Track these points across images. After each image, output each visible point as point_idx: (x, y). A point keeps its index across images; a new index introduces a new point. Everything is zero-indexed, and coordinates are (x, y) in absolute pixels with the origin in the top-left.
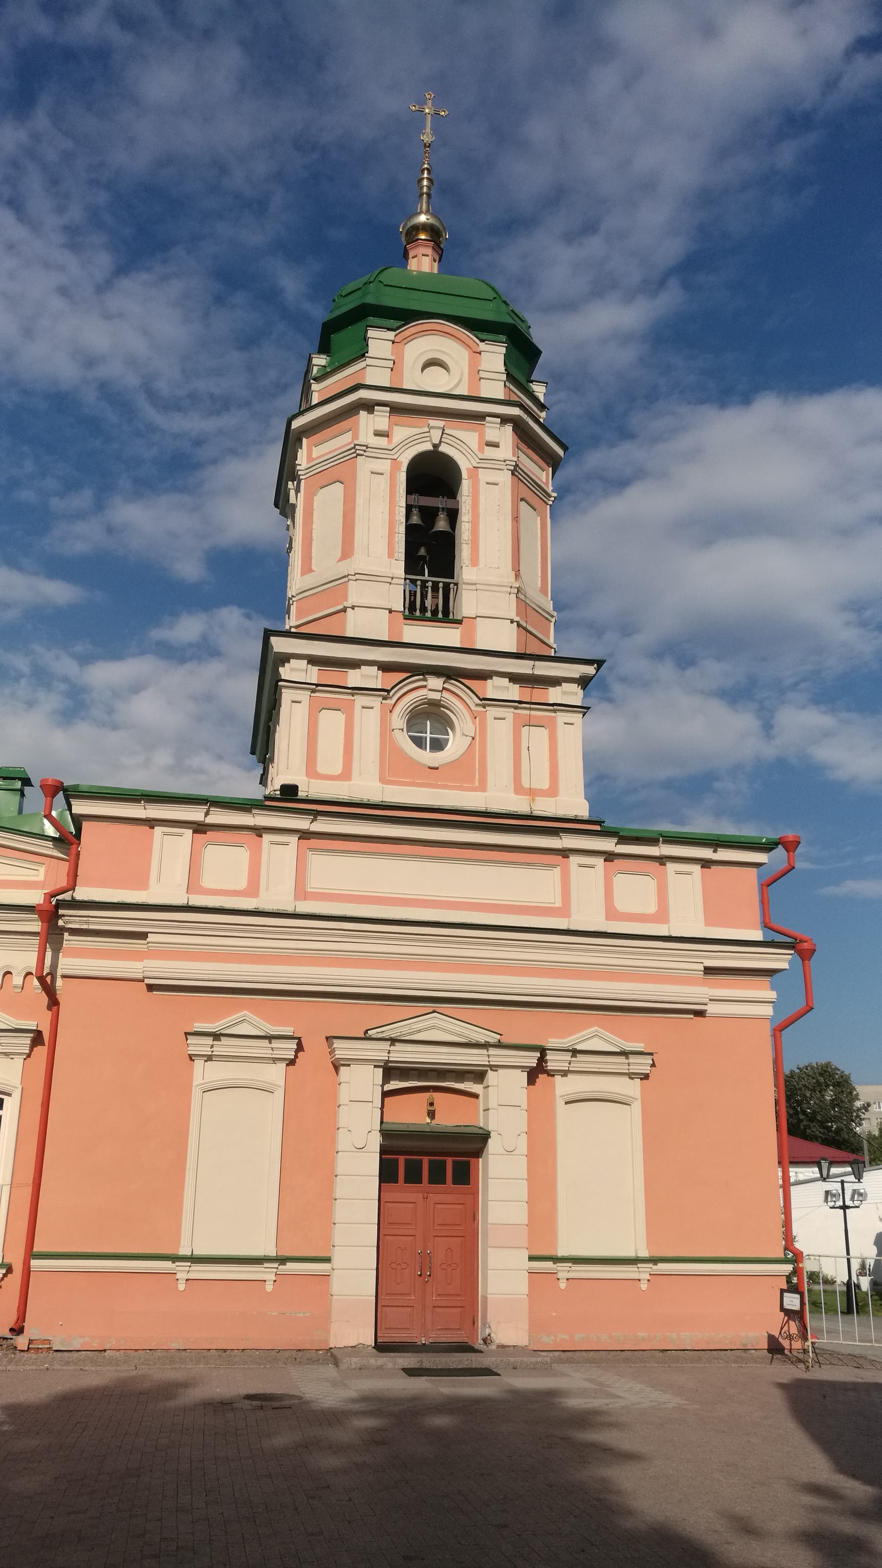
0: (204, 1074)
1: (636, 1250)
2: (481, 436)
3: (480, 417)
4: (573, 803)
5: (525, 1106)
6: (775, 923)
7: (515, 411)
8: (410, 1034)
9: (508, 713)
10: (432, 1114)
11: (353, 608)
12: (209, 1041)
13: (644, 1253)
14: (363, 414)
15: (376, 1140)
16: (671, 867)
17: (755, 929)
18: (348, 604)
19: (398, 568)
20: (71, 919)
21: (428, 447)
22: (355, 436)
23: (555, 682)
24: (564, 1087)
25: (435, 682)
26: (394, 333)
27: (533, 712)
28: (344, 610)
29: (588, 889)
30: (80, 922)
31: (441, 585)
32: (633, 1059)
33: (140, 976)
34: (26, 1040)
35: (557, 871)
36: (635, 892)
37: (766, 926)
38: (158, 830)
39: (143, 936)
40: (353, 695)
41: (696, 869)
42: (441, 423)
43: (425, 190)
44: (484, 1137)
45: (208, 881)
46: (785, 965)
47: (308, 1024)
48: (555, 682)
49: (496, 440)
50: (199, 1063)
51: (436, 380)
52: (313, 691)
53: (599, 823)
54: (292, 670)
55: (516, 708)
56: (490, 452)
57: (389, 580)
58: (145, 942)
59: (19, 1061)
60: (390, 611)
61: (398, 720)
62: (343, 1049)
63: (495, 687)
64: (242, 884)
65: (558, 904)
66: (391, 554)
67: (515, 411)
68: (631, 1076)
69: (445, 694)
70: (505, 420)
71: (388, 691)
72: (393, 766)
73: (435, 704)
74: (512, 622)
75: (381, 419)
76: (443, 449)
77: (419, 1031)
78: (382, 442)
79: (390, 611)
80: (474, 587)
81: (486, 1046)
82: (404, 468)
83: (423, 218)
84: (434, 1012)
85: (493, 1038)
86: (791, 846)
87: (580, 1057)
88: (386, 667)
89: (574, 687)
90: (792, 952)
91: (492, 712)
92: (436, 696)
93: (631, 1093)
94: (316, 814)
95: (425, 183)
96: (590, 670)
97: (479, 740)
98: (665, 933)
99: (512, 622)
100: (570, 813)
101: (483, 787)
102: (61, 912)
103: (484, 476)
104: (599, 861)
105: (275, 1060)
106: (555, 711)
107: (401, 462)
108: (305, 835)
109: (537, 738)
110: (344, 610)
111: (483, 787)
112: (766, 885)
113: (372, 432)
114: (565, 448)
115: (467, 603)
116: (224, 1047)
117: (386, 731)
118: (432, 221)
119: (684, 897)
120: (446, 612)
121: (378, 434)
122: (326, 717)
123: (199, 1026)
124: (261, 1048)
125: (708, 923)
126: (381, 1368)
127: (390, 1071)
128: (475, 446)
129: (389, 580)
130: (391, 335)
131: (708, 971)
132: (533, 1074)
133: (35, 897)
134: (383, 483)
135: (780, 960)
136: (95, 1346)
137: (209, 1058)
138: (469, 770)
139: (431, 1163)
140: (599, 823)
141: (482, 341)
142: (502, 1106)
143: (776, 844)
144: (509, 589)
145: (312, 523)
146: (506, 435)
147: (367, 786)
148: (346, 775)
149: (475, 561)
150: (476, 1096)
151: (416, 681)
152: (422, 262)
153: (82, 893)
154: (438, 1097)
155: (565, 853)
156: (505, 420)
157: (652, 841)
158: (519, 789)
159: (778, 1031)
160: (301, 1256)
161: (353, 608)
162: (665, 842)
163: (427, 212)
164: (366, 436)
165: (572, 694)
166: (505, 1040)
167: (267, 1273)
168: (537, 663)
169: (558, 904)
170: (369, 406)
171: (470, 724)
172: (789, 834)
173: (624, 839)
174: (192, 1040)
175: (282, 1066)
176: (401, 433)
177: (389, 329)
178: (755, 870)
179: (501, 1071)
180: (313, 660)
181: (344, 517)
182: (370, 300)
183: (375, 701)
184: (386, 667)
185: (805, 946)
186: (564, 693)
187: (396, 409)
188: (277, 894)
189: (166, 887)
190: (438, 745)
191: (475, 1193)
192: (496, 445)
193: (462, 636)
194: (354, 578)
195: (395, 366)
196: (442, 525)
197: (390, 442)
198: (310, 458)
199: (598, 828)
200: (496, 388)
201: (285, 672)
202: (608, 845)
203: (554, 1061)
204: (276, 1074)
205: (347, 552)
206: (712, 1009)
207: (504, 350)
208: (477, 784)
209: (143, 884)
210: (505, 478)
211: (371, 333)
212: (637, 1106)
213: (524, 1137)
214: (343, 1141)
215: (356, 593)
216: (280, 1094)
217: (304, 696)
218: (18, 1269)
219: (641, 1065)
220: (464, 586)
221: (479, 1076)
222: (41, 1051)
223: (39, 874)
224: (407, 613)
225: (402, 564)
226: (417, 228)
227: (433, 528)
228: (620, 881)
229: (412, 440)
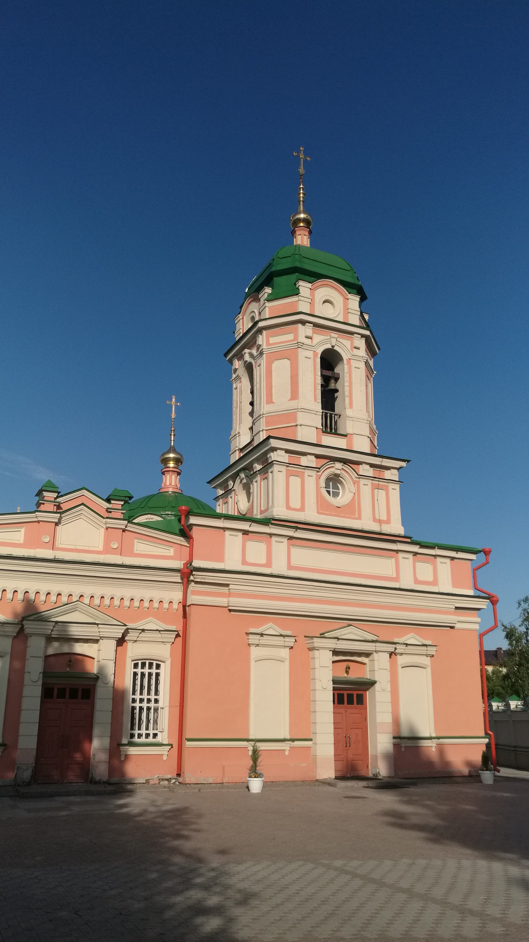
0: (255, 652)
1: (430, 734)
2: (352, 343)
3: (352, 333)
4: (396, 527)
5: (389, 670)
6: (479, 586)
7: (367, 333)
8: (342, 635)
9: (369, 482)
10: (347, 672)
11: (301, 425)
12: (258, 637)
13: (434, 735)
14: (300, 325)
15: (331, 686)
16: (439, 560)
17: (471, 589)
18: (299, 423)
19: (318, 407)
20: (198, 576)
21: (329, 346)
22: (296, 337)
23: (388, 468)
24: (401, 660)
25: (338, 465)
26: (311, 285)
27: (380, 483)
28: (296, 426)
29: (409, 569)
30: (201, 578)
31: (329, 414)
32: (429, 648)
33: (226, 605)
34: (173, 635)
35: (393, 559)
36: (425, 570)
37: (476, 588)
38: (227, 533)
39: (227, 585)
40: (304, 469)
41: (448, 561)
42: (336, 336)
43: (302, 199)
44: (372, 683)
45: (249, 559)
46: (485, 607)
47: (304, 630)
48: (388, 468)
49: (359, 346)
50: (253, 648)
51: (328, 311)
52: (288, 466)
53: (410, 538)
54: (278, 455)
55: (372, 480)
56: (356, 352)
57: (316, 413)
58: (227, 588)
59: (169, 646)
60: (317, 428)
61: (323, 484)
62: (318, 642)
63: (364, 470)
64: (264, 561)
65: (395, 576)
66: (315, 400)
67: (367, 333)
68: (427, 655)
69: (342, 472)
70: (363, 336)
71: (319, 468)
72: (323, 507)
73: (337, 476)
74: (368, 437)
75: (308, 330)
76: (336, 348)
77: (345, 635)
78: (308, 341)
79: (317, 428)
80: (351, 419)
81: (373, 641)
82: (319, 357)
83: (302, 216)
84: (351, 625)
85: (375, 638)
86: (487, 553)
87: (409, 647)
88: (318, 456)
89: (396, 471)
90: (488, 601)
91: (362, 481)
92: (338, 472)
93: (426, 663)
94: (297, 528)
95: (302, 195)
96: (404, 464)
97: (357, 494)
98: (437, 591)
99: (368, 437)
100: (393, 532)
101: (359, 518)
102: (194, 573)
103: (354, 363)
104: (410, 556)
105: (285, 647)
106: (388, 482)
107: (318, 353)
108: (291, 538)
109: (382, 494)
110: (296, 426)
111: (359, 518)
112: (475, 570)
113: (304, 336)
114: (379, 349)
115: (348, 426)
116: (265, 640)
117: (318, 488)
118: (305, 216)
119: (443, 573)
120: (336, 430)
121: (307, 337)
122: (292, 478)
123: (252, 630)
124: (280, 641)
125: (454, 586)
126: (352, 787)
127: (335, 653)
128: (349, 348)
129: (316, 413)
130: (310, 285)
131: (457, 608)
132: (391, 654)
133: (178, 564)
134: (310, 362)
135: (483, 604)
136: (218, 781)
137: (258, 645)
138: (352, 509)
139: (350, 695)
140: (410, 538)
141: (350, 293)
142: (378, 668)
143: (481, 551)
144: (366, 421)
145: (272, 377)
146: (361, 343)
147: (311, 515)
148: (302, 509)
149: (351, 406)
150: (364, 664)
151: (331, 464)
152: (302, 239)
153: (196, 563)
154: (350, 664)
155: (397, 551)
156: (363, 336)
157: (432, 548)
158: (375, 520)
159: (481, 636)
160: (301, 737)
161: (301, 425)
162: (438, 548)
163: (304, 212)
164: (302, 339)
165: (393, 475)
166: (380, 639)
167: (286, 747)
168: (384, 459)
169: (395, 576)
170: (303, 322)
171: (353, 486)
172: (487, 547)
173: (422, 546)
174: (251, 636)
175: (288, 649)
176: (318, 338)
177: (309, 282)
178: (470, 562)
179: (380, 653)
180: (287, 451)
181: (292, 377)
182: (298, 264)
183: (313, 473)
184: (318, 456)
185: (494, 599)
186: (392, 474)
187: (316, 325)
188: (279, 567)
189: (232, 562)
190: (336, 495)
191: (366, 708)
192: (358, 349)
193: (347, 443)
194: (300, 410)
195: (312, 303)
196: (332, 386)
197: (312, 342)
198: (268, 344)
199: (409, 540)
200: (355, 319)
201: (273, 456)
202: (415, 548)
203: (400, 649)
204: (285, 653)
205: (295, 395)
206: (458, 626)
207: (359, 299)
208: (357, 516)
209: (221, 559)
210: (362, 365)
211: (301, 283)
212: (429, 670)
213: (389, 683)
214: (318, 685)
215: (301, 418)
216: (287, 663)
217: (283, 468)
218: (176, 746)
219: (432, 651)
220: (347, 418)
221: (367, 655)
222: (180, 640)
223: (171, 551)
224: (324, 430)
225: (320, 405)
226: (299, 220)
227: (328, 387)
228: (420, 566)
229: (322, 342)
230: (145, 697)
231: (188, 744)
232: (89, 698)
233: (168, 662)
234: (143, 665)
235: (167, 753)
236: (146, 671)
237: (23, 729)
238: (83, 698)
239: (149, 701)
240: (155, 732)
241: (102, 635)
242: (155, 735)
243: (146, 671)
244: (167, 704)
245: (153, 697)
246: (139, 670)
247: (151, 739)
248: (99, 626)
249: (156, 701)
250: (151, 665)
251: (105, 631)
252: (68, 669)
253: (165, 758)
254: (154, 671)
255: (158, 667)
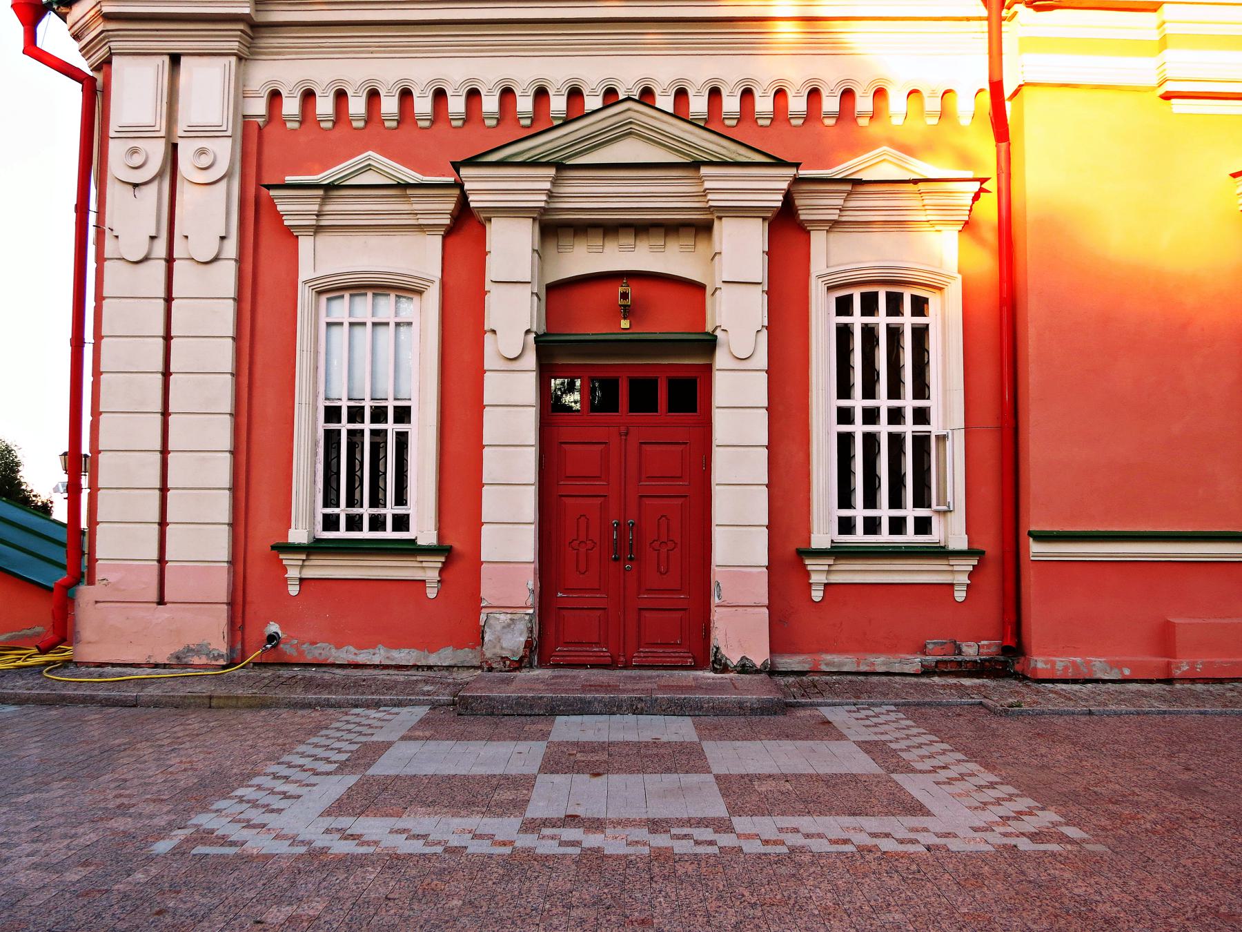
230: (883, 402)
231: (1037, 549)
232: (693, 409)
233: (954, 292)
234: (869, 306)
235: (964, 579)
236: (882, 320)
237: (492, 504)
238: (673, 407)
239: (896, 416)
240: (922, 512)
241: (716, 200)
242: (923, 526)
243: (882, 320)
244: (958, 420)
245: (908, 403)
246: (857, 320)
247: (910, 536)
248: (704, 171)
249: (921, 416)
250: (894, 306)
251: (722, 186)
252: (625, 324)
253: (960, 595)
254: (907, 320)
255: (920, 306)
